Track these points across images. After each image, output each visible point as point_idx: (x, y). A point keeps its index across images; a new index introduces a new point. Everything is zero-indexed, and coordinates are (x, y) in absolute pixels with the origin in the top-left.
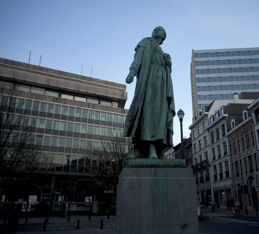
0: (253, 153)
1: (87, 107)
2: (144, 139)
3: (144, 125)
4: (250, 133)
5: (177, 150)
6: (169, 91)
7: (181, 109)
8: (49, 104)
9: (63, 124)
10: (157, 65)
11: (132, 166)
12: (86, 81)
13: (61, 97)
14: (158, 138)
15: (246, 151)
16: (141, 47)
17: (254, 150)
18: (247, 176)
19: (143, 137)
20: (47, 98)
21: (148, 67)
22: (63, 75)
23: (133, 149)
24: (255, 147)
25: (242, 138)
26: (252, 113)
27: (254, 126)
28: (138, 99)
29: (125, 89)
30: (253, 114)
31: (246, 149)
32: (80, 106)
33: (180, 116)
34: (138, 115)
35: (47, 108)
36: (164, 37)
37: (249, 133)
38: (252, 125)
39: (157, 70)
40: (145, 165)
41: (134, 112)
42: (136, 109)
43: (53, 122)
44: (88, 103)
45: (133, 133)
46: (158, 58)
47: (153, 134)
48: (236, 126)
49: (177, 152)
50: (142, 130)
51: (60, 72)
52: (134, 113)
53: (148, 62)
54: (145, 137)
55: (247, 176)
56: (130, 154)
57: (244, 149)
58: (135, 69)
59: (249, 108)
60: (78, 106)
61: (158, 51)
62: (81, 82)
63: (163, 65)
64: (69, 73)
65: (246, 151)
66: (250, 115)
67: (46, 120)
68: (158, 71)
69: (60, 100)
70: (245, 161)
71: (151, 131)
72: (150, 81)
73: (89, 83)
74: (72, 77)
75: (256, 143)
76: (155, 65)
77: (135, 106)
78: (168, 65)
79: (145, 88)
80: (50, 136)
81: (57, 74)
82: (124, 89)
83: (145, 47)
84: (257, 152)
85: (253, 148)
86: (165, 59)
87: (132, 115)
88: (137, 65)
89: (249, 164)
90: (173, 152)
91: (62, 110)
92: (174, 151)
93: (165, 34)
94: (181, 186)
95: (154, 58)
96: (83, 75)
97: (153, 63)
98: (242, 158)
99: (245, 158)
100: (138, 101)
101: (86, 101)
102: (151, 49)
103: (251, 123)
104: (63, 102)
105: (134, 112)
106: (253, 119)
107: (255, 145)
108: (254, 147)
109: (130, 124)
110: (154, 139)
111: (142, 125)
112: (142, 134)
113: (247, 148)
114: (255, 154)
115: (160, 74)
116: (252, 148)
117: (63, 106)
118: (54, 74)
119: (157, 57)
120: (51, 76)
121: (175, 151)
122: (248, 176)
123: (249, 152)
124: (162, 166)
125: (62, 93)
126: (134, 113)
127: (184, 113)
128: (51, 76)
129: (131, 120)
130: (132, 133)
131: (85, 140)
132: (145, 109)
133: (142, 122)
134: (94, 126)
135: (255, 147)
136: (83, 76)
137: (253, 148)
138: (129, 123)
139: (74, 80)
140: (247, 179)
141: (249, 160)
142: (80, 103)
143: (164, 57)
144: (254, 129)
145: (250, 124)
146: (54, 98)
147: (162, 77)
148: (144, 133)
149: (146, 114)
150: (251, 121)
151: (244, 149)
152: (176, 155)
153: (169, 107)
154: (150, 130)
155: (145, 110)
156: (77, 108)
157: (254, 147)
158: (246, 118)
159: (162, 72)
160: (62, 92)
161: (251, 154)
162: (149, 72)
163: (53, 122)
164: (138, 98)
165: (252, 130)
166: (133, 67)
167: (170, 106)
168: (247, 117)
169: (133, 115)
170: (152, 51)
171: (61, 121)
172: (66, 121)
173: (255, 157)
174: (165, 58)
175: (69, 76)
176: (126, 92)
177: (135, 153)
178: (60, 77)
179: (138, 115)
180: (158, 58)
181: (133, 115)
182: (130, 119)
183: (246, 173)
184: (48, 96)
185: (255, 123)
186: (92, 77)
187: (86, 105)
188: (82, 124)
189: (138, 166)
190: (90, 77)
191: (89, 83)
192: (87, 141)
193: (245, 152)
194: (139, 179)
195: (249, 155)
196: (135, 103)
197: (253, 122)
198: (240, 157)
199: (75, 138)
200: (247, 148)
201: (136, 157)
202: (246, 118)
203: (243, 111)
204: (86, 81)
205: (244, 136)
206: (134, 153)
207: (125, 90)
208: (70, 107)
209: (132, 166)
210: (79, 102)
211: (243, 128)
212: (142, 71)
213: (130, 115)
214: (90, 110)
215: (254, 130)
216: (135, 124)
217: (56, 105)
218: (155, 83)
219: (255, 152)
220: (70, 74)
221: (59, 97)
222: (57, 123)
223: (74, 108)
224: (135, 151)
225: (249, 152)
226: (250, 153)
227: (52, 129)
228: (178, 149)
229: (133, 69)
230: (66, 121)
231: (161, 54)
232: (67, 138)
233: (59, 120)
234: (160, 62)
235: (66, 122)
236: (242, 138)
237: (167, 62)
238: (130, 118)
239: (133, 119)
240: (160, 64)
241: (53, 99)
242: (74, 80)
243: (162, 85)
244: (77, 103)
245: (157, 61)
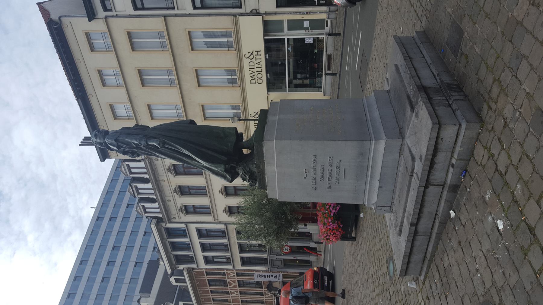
0: (236, 277)
4: (206, 278)
15: (230, 289)
17: (233, 275)
18: (266, 294)
24: (229, 272)
25: (212, 292)
26: (178, 267)
27: (199, 269)
30: (181, 267)
31: (229, 287)
37: (206, 279)
38: (195, 272)
48: (191, 301)
55: (266, 294)
57: (227, 293)
59: (169, 272)
65: (230, 289)
66: (181, 273)
70: (245, 293)
75: (223, 269)
84: (235, 271)
85: (229, 276)
89: (250, 287)
98: (240, 298)
99: (241, 293)
103: (193, 273)
106: (188, 268)
107: (225, 271)
108: (228, 275)
113: (227, 286)
114: (238, 275)
116: (228, 278)
122: (267, 292)
123: (234, 284)
135: (229, 272)
137: (229, 276)
140: (270, 295)
141: (244, 287)
144: (202, 269)
145: (194, 274)
150: (190, 271)
151: (227, 293)
157: (228, 275)
158: (184, 281)
161: (237, 281)
165: (202, 273)
168: (183, 278)
173: (242, 275)
183: (261, 294)
185: (194, 266)
193: (232, 291)
195: (237, 284)
197: (193, 269)
198: (238, 302)
200: (227, 286)
202: (184, 281)
203: (170, 283)
205: (209, 288)
211: (197, 288)
215: (204, 270)
219: (235, 274)
225: (234, 284)
226: (234, 282)
236: (212, 292)
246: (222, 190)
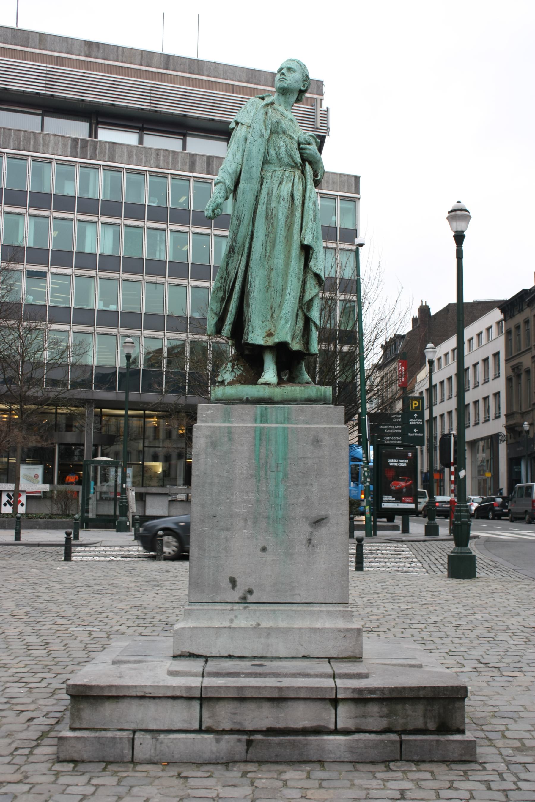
1: (187, 167)
2: (249, 341)
3: (250, 310)
5: (512, 316)
6: (306, 230)
7: (459, 202)
8: (60, 162)
9: (110, 231)
10: (281, 167)
11: (218, 401)
12: (179, 74)
13: (96, 137)
14: (277, 340)
16: (242, 124)
19: (247, 337)
20: (52, 143)
21: (257, 176)
22: (100, 55)
23: (231, 361)
28: (236, 252)
29: (320, 97)
32: (162, 164)
33: (454, 224)
34: (237, 287)
35: (54, 177)
36: (304, 86)
39: (280, 179)
40: (245, 398)
41: (229, 280)
42: (233, 273)
43: (76, 224)
44: (192, 156)
45: (227, 329)
46: (283, 150)
47: (270, 330)
49: (513, 323)
50: (247, 320)
51: (89, 44)
52: (228, 282)
53: (256, 162)
54: (251, 335)
56: (224, 372)
58: (225, 183)
60: (157, 167)
61: (284, 132)
62: (162, 77)
63: (295, 166)
64: (118, 47)
67: (52, 221)
68: (281, 183)
69: (95, 149)
71: (265, 323)
72: (261, 209)
73: (189, 81)
74: (131, 63)
76: (275, 169)
77: (229, 268)
78: (311, 163)
79: (251, 224)
80: (70, 275)
81: (79, 55)
82: (315, 96)
83: (250, 126)
86: (300, 149)
87: (224, 287)
88: (230, 174)
90: (501, 321)
91: (102, 183)
92: (502, 316)
93: (304, 78)
94: (316, 442)
95: (272, 152)
96: (168, 51)
97: (270, 163)
100: (236, 255)
101: (184, 147)
102: (266, 130)
104: (104, 156)
105: (229, 280)
109: (221, 306)
110: (270, 342)
111: (245, 310)
112: (246, 329)
115: (286, 188)
117: (107, 168)
118: (68, 53)
119: (279, 148)
120: (59, 61)
121: (505, 316)
124: (281, 401)
125: (98, 123)
126: (228, 282)
127: (471, 214)
128: (59, 61)
129: (223, 299)
130: (224, 327)
131: (185, 286)
132: (251, 275)
133: (245, 302)
134: (216, 236)
136: (169, 56)
138: (219, 305)
139: (138, 73)
142: (164, 156)
143: (299, 144)
146: (75, 141)
147: (292, 196)
148: (250, 327)
149: (253, 285)
152: (508, 333)
153: (306, 265)
155: (252, 278)
156: (153, 174)
159: (291, 185)
160: (100, 119)
162: (262, 185)
163: (76, 224)
164: (236, 249)
166: (222, 180)
167: (312, 264)
169: (227, 287)
170: (266, 135)
171: (103, 223)
172: (118, 221)
174: (302, 146)
175: (120, 58)
176: (324, 108)
177: (234, 370)
178: (88, 65)
179: (237, 287)
180: (283, 150)
181: (227, 287)
182: (221, 295)
184: (55, 135)
186: (201, 58)
187: (184, 163)
188: (172, 231)
189: (229, 400)
190: (193, 56)
191: (189, 81)
192: (193, 287)
194: (228, 427)
196: (230, 262)
199: (153, 279)
201: (235, 379)
204: (179, 74)
206: (232, 371)
207: (321, 100)
208: (130, 171)
209: (218, 401)
210: (158, 151)
212: (241, 186)
213: (220, 287)
214: (198, 180)
216: (231, 308)
217: (84, 166)
218: (274, 212)
220: (123, 53)
221: (90, 136)
222: (89, 229)
223: (142, 173)
224: (233, 367)
227: (75, 250)
228: (516, 313)
229: (221, 184)
230: (118, 221)
231: (292, 138)
232: (124, 280)
233: (94, 219)
234: (286, 159)
235: (119, 225)
237: (306, 155)
238: (221, 294)
239: (227, 295)
240: (288, 165)
241: (69, 147)
242: (138, 73)
243: (290, 216)
244: (154, 155)
245: (279, 158)
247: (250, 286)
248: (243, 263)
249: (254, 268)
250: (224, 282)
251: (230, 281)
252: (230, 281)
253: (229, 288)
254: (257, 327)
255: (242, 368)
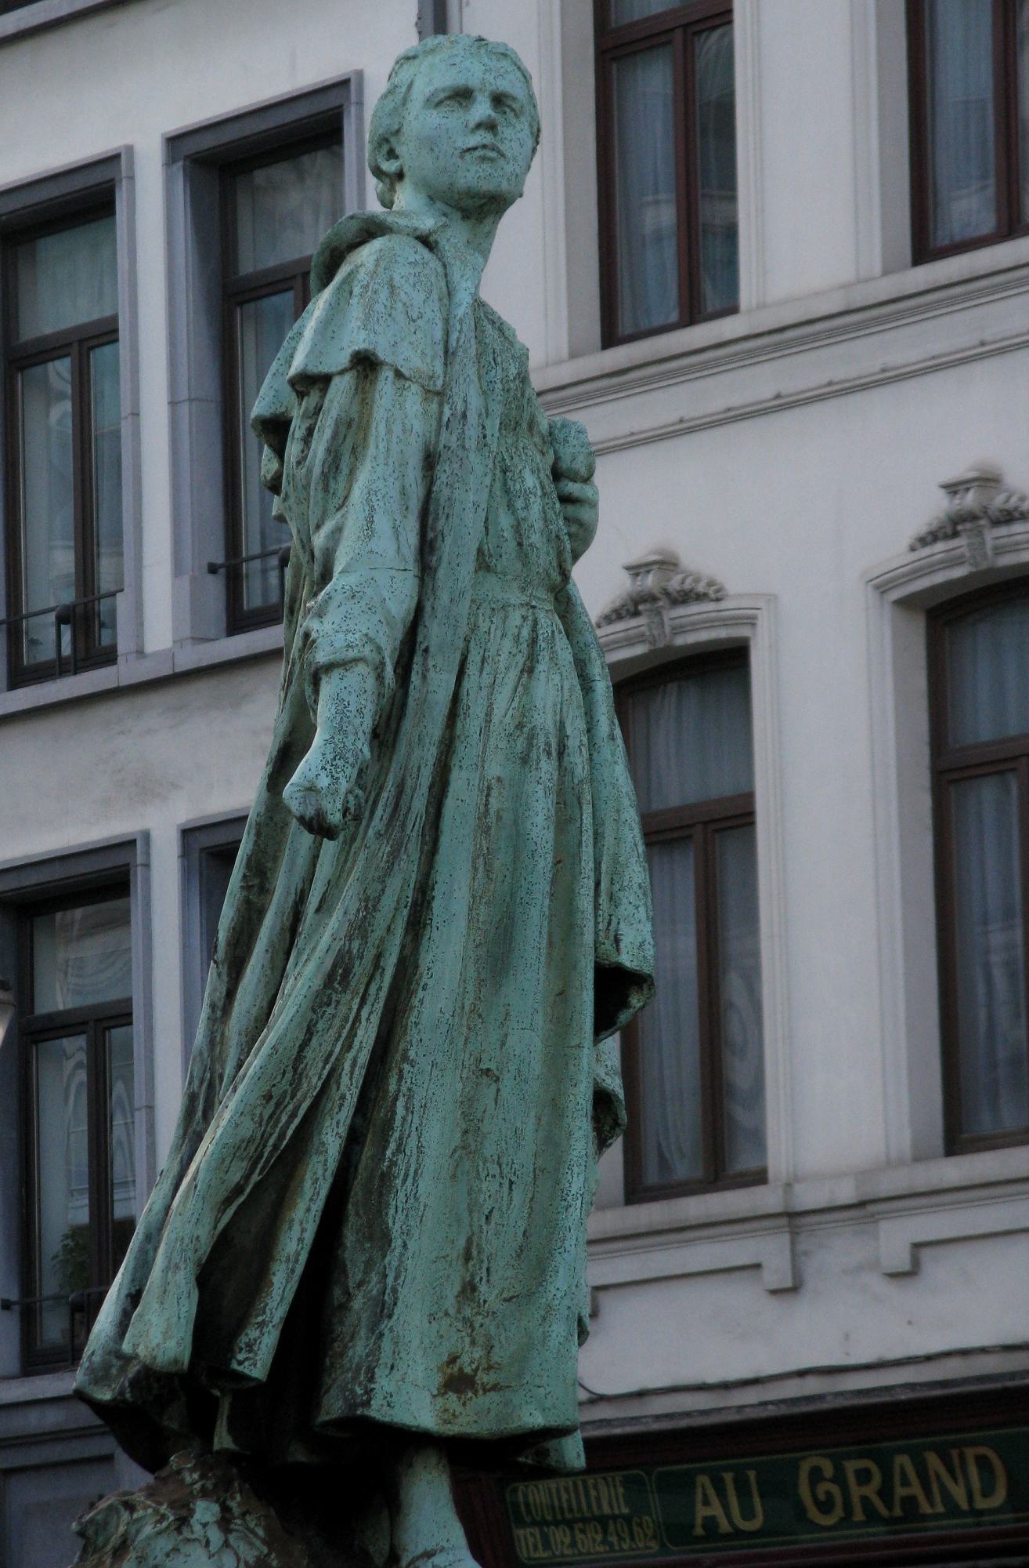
2: (377, 1411)
3: (392, 1259)
16: (399, 374)
19: (369, 1392)
42: (313, 1081)
47: (453, 1360)
52: (284, 1119)
54: (384, 1383)
77: (309, 1054)
95: (505, 521)
126: (284, 1119)
130: (252, 1333)
132: (410, 1098)
148: (386, 1345)
149: (412, 1143)
154: (432, 1317)
166: (367, 651)
177: (232, 1538)
196: (320, 1026)
206: (226, 1544)
218: (494, 804)
224: (225, 1523)
239: (255, 1178)
246: (686, 597)
247: (400, 1149)
248: (367, 1036)
249: (424, 1064)
250: (271, 1117)
251: (293, 1115)
252: (293, 1115)
253: (275, 1147)
254: (416, 1343)
255: (261, 1532)
